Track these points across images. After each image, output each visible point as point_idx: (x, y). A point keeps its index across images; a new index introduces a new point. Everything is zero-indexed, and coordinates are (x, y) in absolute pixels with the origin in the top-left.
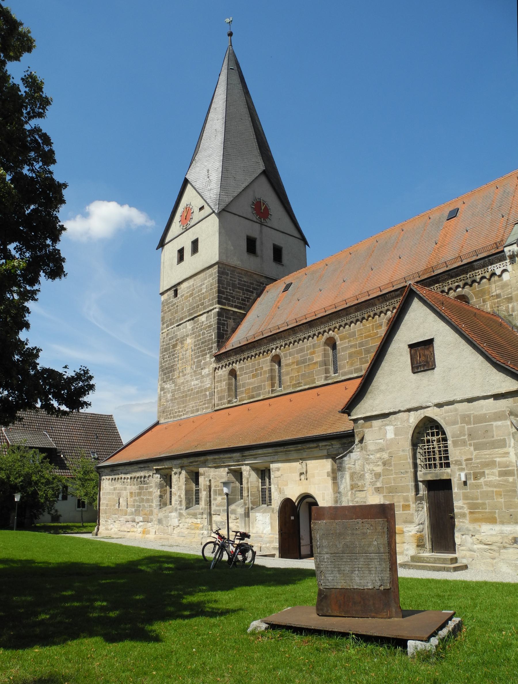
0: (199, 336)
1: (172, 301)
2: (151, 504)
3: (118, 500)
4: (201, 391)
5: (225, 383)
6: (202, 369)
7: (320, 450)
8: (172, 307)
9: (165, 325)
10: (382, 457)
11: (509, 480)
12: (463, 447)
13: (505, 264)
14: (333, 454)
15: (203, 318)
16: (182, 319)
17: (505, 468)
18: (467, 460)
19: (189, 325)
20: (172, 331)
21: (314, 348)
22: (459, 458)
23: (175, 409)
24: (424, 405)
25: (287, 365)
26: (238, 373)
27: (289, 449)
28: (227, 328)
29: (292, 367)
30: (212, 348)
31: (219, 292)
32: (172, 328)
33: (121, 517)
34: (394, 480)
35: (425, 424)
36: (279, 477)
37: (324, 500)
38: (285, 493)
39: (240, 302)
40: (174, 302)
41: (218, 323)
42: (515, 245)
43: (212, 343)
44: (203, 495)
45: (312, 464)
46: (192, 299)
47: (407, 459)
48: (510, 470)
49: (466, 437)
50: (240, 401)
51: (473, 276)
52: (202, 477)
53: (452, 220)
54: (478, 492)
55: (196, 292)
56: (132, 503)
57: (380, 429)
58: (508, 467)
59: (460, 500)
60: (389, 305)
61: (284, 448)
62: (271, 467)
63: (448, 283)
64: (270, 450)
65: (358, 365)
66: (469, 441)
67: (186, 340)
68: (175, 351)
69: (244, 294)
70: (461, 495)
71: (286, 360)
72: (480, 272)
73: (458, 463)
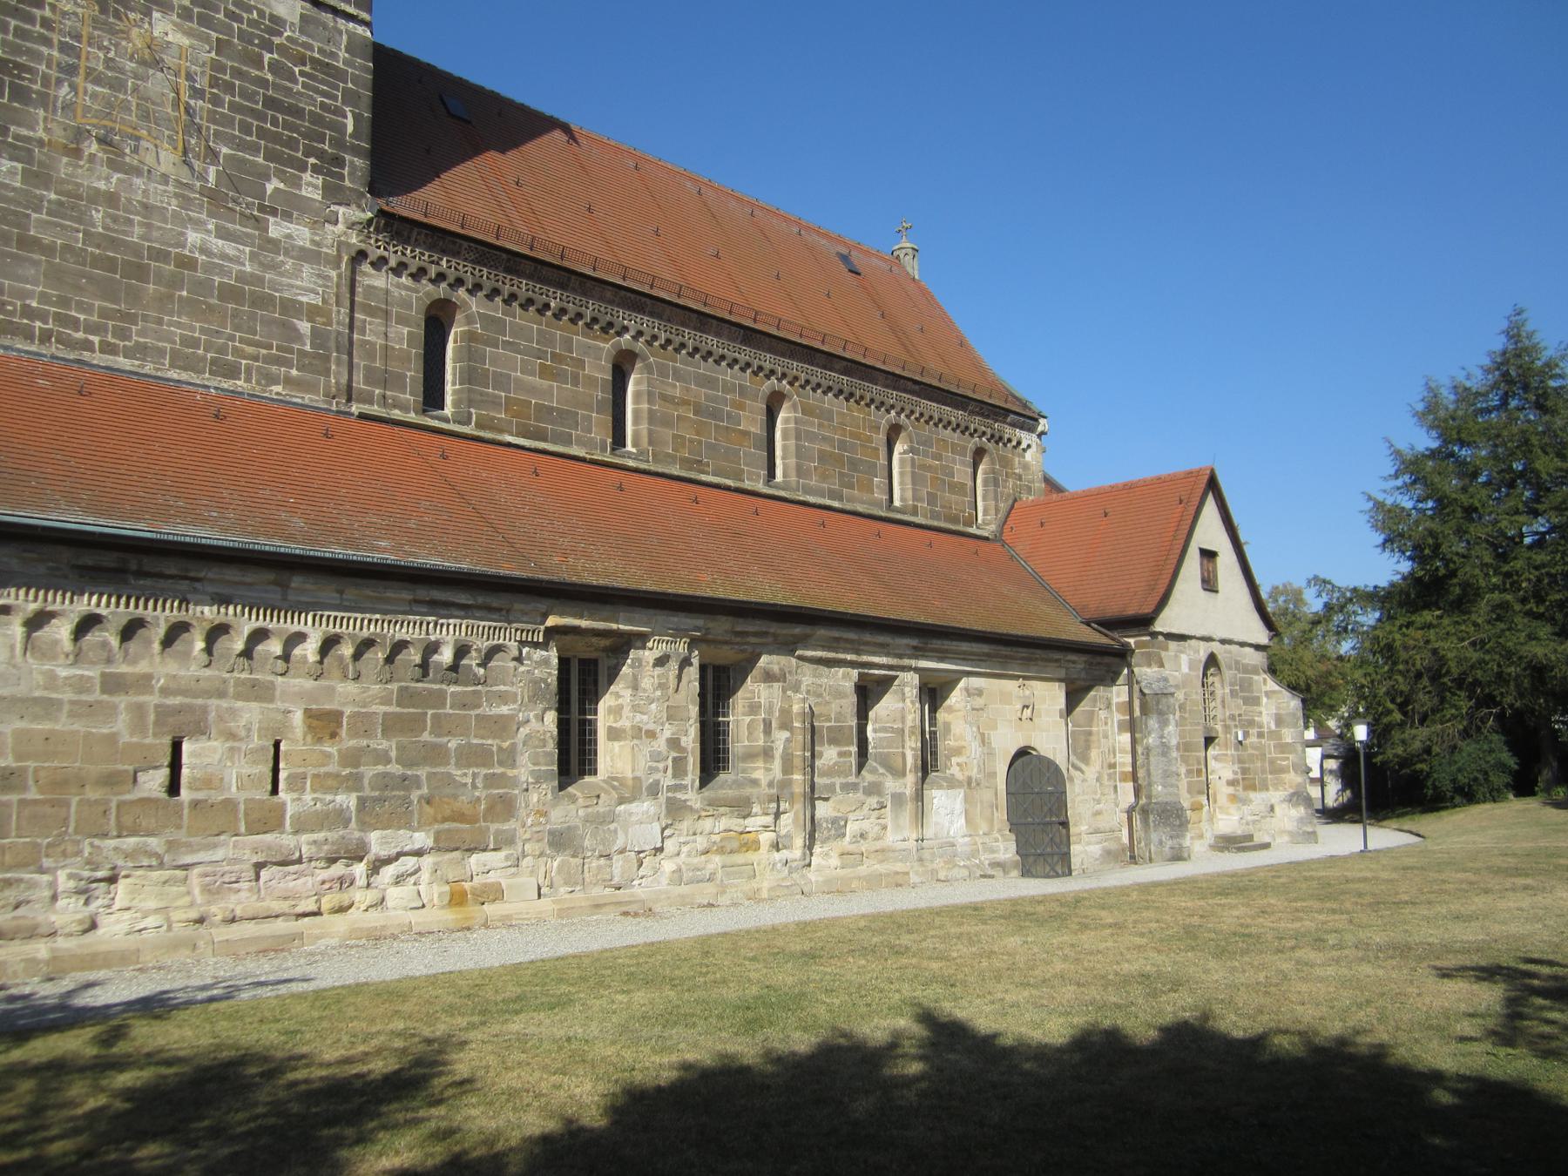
2: (499, 770)
29: (681, 411)
64: (985, 648)
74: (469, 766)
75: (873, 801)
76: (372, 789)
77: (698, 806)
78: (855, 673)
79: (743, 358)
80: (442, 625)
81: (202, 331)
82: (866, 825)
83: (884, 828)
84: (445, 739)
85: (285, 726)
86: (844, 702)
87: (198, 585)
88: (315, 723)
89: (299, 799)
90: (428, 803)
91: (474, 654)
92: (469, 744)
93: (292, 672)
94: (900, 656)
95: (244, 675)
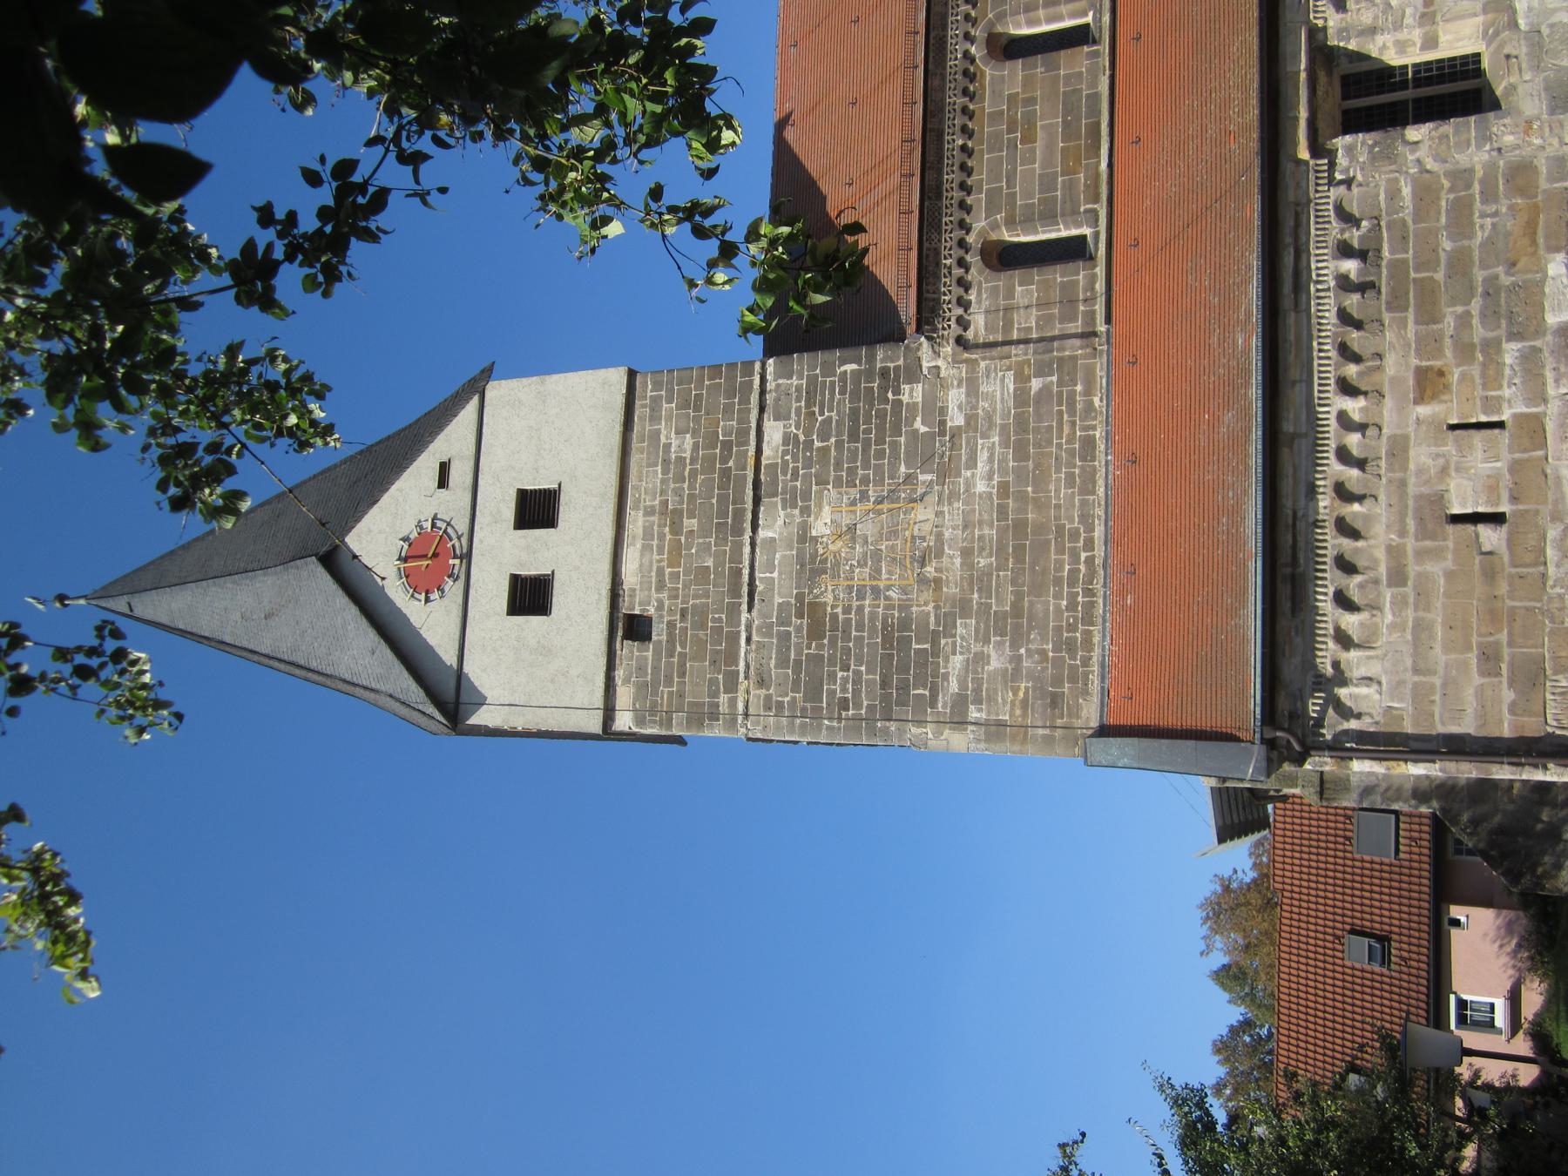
2: (1477, 187)
74: (1472, 224)
76: (1499, 327)
80: (1318, 275)
81: (1058, 471)
84: (1442, 254)
85: (1433, 422)
87: (1300, 514)
88: (1429, 392)
89: (1509, 401)
90: (1514, 264)
91: (1346, 235)
92: (1447, 227)
93: (1377, 420)
95: (1383, 464)
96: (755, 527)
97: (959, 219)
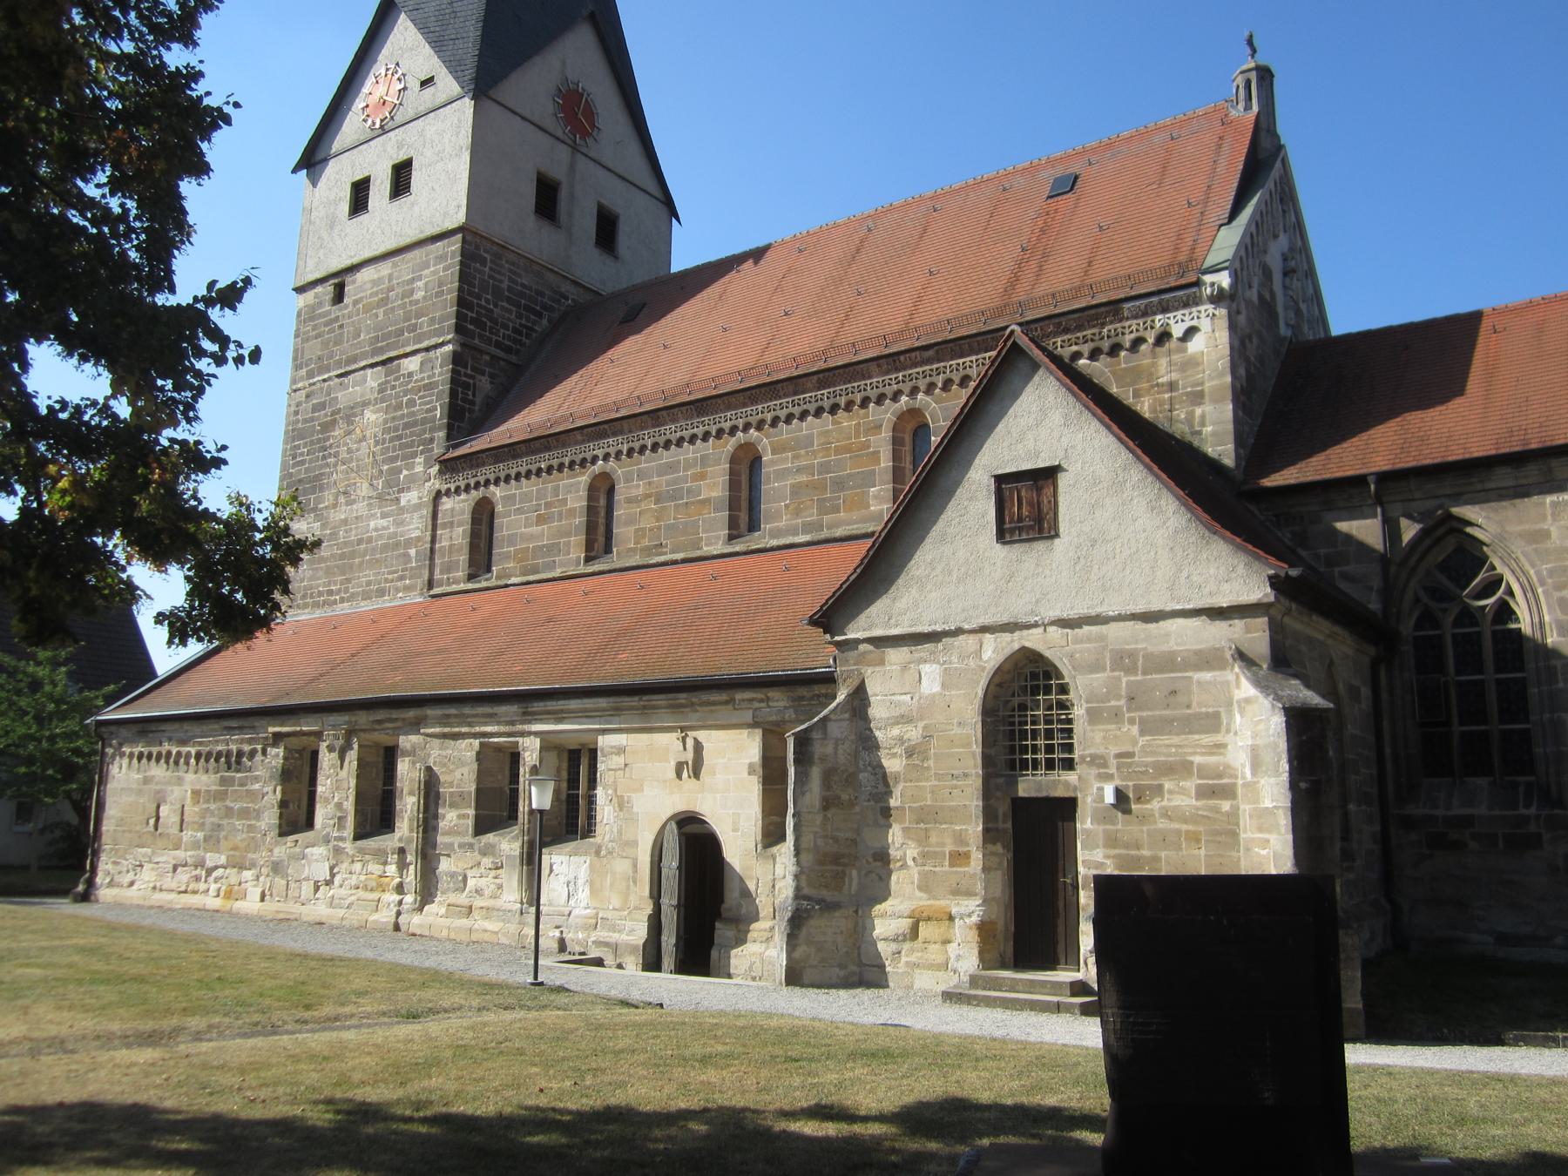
0: (399, 407)
1: (329, 313)
2: (253, 822)
3: (155, 809)
4: (397, 545)
5: (461, 529)
6: (401, 491)
7: (735, 709)
8: (325, 325)
9: (303, 372)
10: (905, 737)
11: (1220, 808)
12: (1113, 726)
13: (1195, 314)
14: (767, 722)
15: (412, 364)
16: (354, 359)
17: (1213, 779)
18: (1119, 756)
19: (373, 379)
20: (322, 388)
21: (703, 465)
22: (1101, 751)
23: (318, 586)
24: (1023, 619)
25: (629, 501)
26: (499, 508)
27: (654, 703)
28: (474, 395)
29: (643, 506)
30: (432, 440)
31: (462, 302)
32: (324, 380)
33: (163, 855)
34: (932, 792)
35: (1016, 664)
36: (620, 769)
37: (735, 830)
38: (635, 810)
39: (509, 336)
40: (333, 316)
41: (454, 381)
42: (1226, 273)
43: (432, 430)
44: (408, 805)
45: (713, 740)
46: (385, 313)
47: (969, 745)
48: (1226, 785)
49: (1122, 702)
50: (498, 578)
51: (1117, 335)
52: (407, 759)
53: (1060, 198)
54: (1142, 831)
55: (397, 296)
56: (196, 819)
57: (905, 668)
58: (1220, 776)
59: (1098, 847)
60: (903, 382)
61: (641, 700)
62: (600, 744)
63: (1054, 343)
64: (602, 702)
65: (812, 515)
66: (1129, 710)
67: (362, 414)
68: (328, 439)
69: (520, 316)
70: (1101, 836)
71: (628, 487)
72: (1134, 328)
73: (1098, 761)
75: (487, 862)
77: (351, 853)
78: (476, 743)
79: (700, 431)
82: (483, 882)
83: (500, 887)
86: (465, 770)
94: (512, 723)
96: (372, 366)
97: (970, 374)
